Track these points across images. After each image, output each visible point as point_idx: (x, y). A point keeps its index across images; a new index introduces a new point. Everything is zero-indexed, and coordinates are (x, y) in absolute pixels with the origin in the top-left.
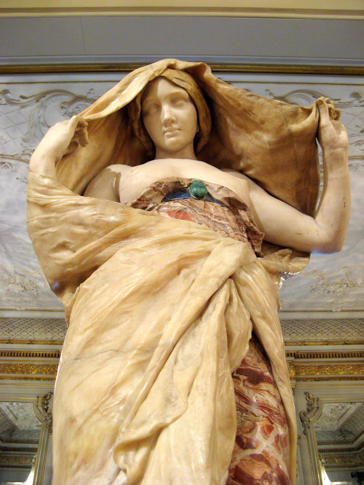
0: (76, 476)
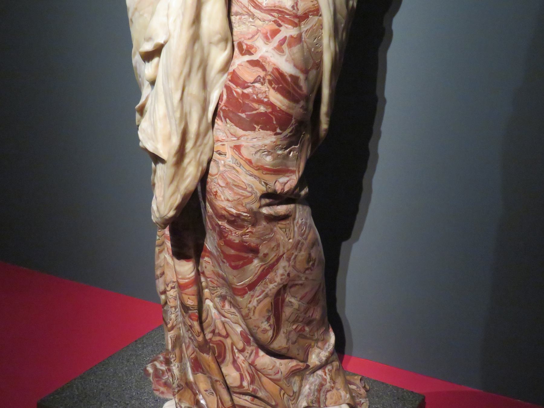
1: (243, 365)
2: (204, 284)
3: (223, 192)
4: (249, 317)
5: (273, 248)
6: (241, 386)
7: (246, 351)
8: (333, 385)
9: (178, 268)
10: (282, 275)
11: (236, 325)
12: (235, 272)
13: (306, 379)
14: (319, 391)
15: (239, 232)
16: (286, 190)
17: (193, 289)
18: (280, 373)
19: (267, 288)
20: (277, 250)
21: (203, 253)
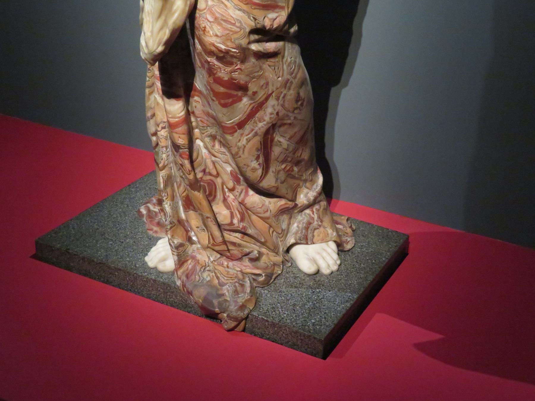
1: (233, 204)
2: (194, 124)
3: (211, 27)
5: (262, 86)
6: (231, 224)
7: (236, 190)
8: (320, 223)
9: (167, 107)
10: (271, 114)
11: (226, 164)
12: (225, 110)
13: (295, 218)
14: (307, 228)
15: (229, 69)
16: (275, 26)
17: (183, 128)
18: (269, 211)
19: (257, 126)
21: (193, 93)
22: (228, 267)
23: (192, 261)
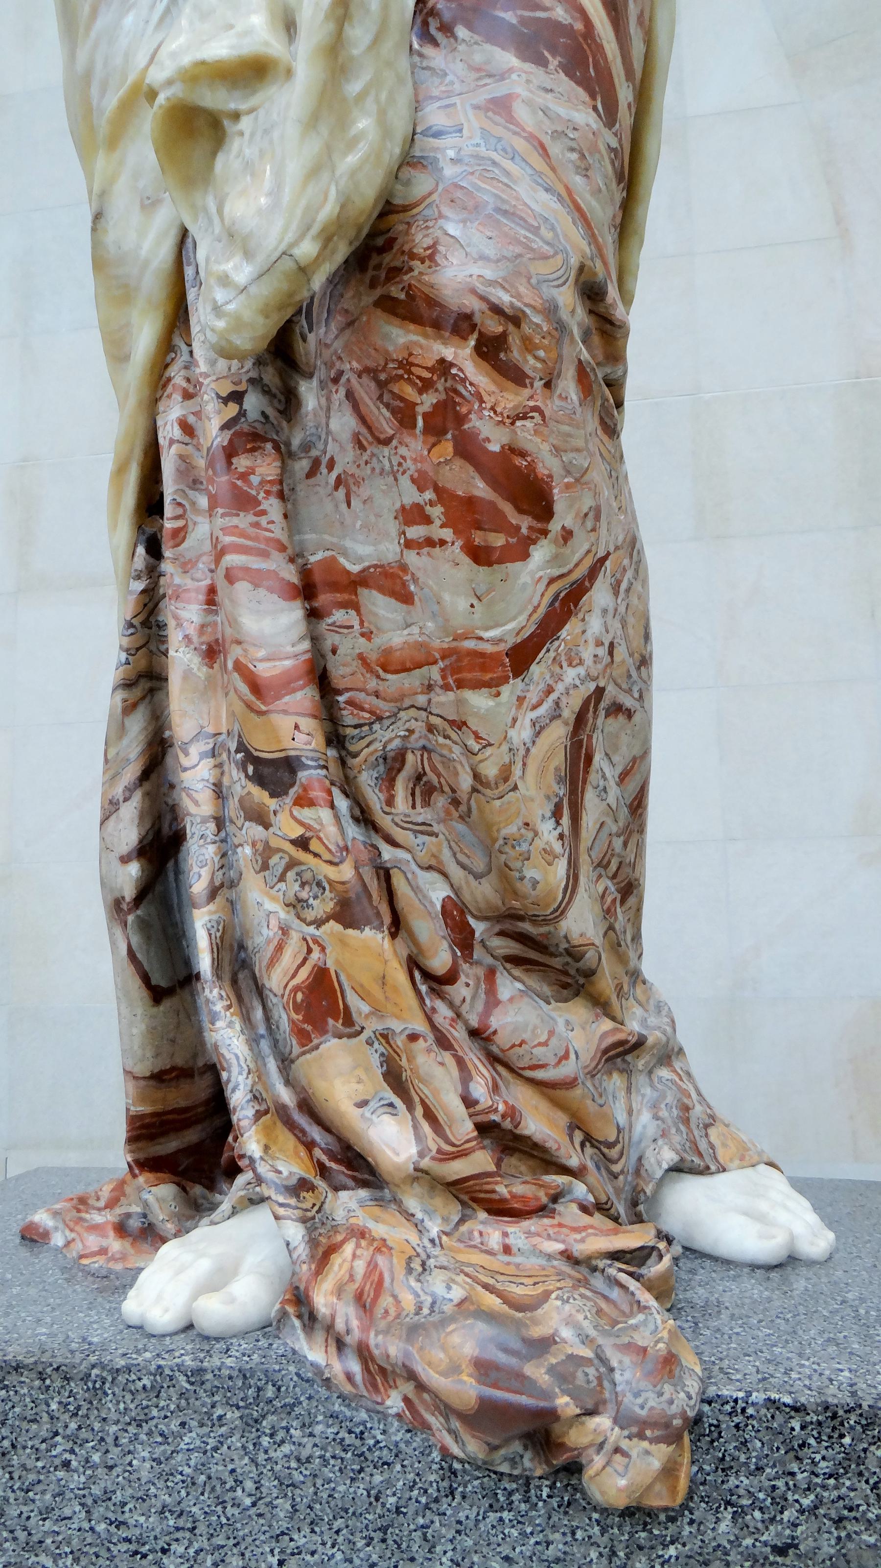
0: (93, 34)
4: (510, 783)
5: (586, 515)
7: (463, 979)
11: (433, 876)
13: (638, 1091)
20: (593, 530)
22: (507, 1250)
23: (358, 1246)
